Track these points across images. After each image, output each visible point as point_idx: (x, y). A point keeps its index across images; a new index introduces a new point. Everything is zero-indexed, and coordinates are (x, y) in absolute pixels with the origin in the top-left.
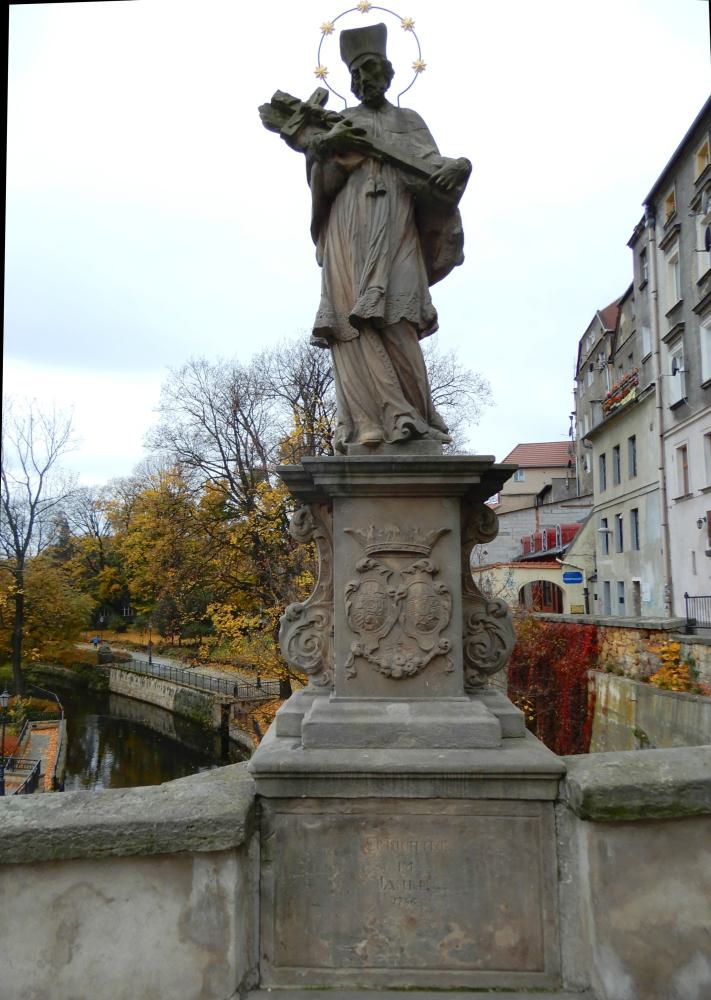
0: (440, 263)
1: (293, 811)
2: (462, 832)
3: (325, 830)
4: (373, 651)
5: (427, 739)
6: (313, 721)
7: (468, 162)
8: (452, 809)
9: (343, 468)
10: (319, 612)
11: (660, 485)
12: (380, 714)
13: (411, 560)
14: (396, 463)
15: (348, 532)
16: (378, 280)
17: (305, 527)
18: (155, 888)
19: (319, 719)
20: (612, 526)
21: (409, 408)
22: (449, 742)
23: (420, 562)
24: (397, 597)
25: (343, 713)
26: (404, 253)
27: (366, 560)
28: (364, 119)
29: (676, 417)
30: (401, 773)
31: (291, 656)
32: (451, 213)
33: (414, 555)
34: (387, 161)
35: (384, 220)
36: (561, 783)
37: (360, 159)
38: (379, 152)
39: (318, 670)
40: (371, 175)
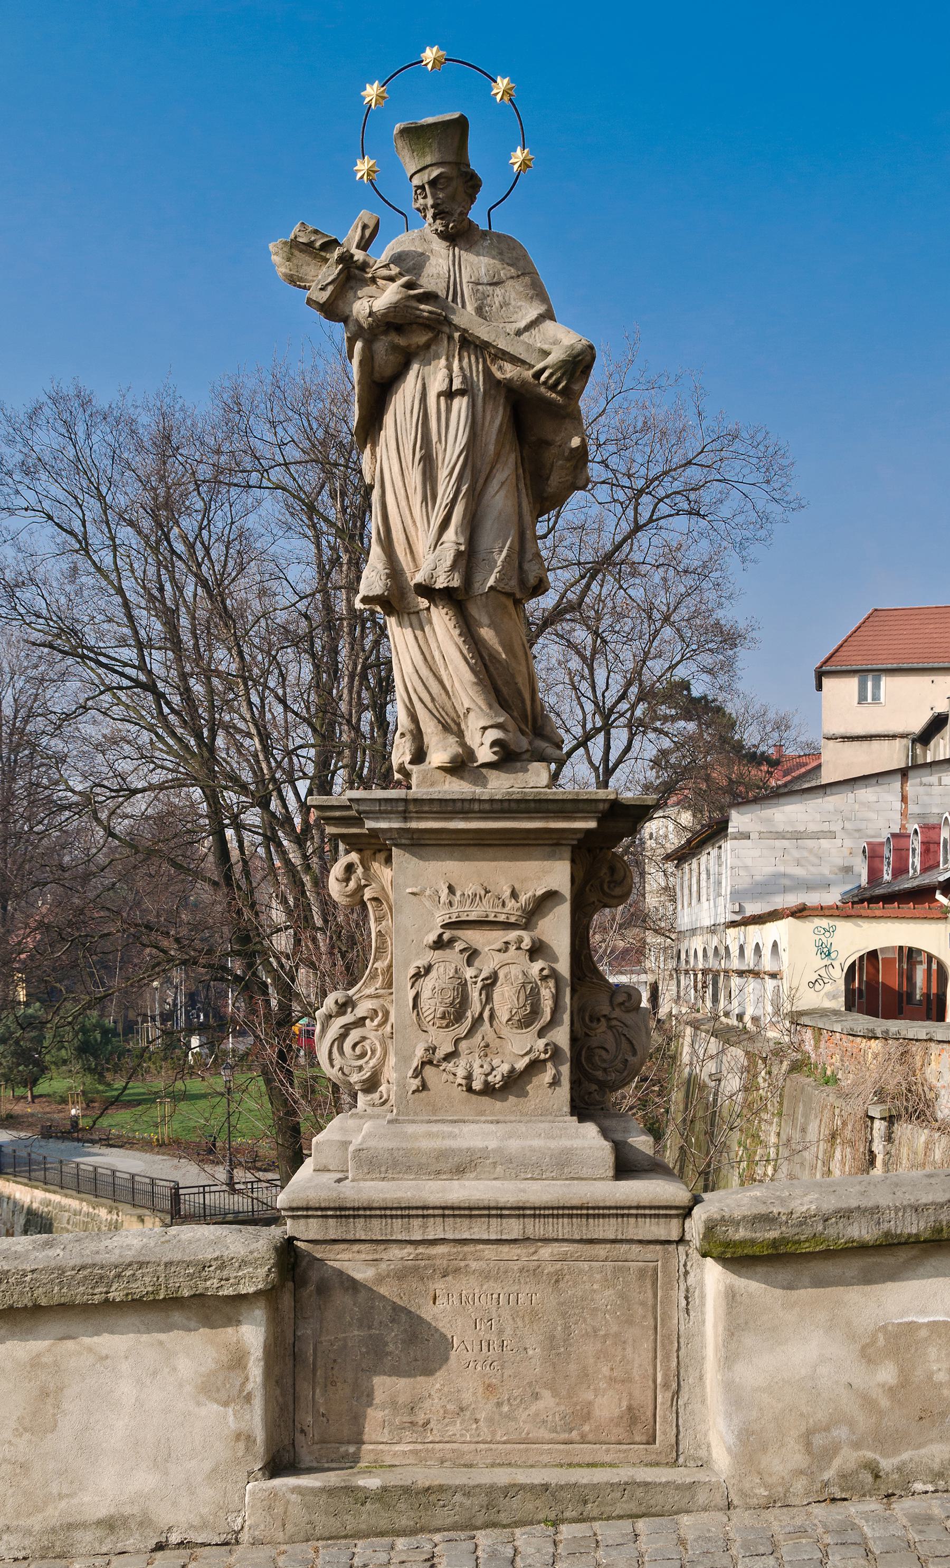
13: (501, 933)
14: (480, 801)
15: (413, 894)
17: (352, 884)
39: (371, 1085)
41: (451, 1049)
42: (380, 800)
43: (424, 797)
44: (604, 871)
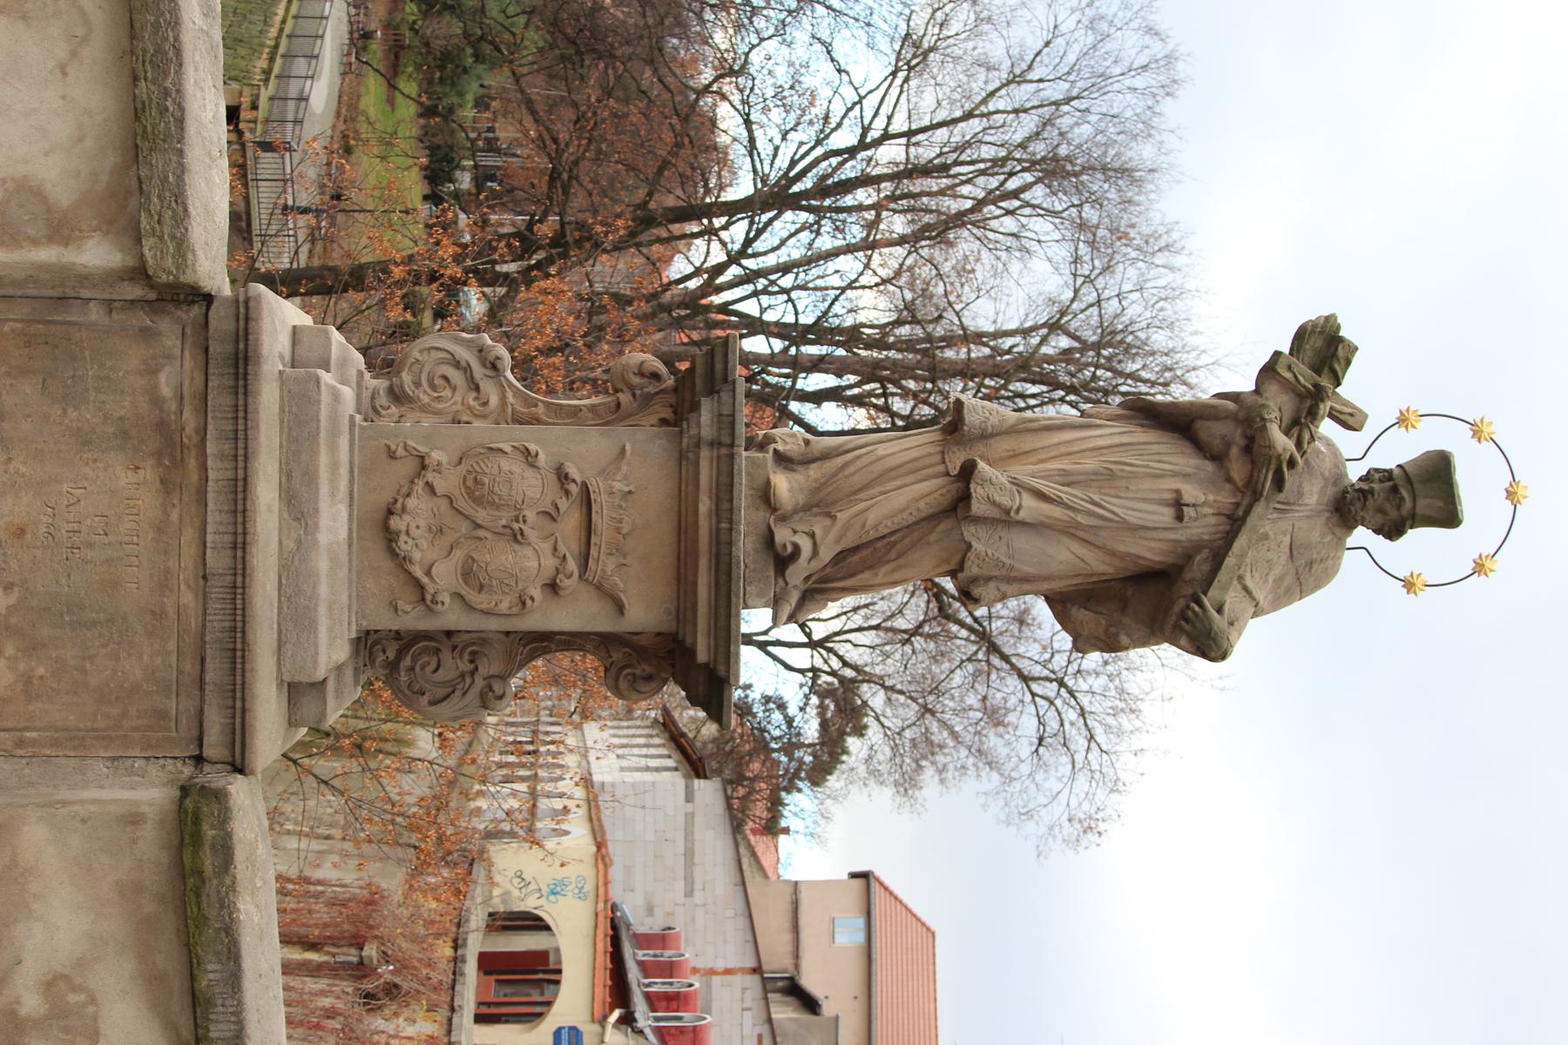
0: (1079, 614)
1: (187, 353)
2: (153, 613)
3: (157, 401)
4: (430, 488)
5: (294, 570)
6: (323, 388)
7: (1223, 657)
8: (188, 599)
9: (724, 445)
10: (494, 400)
12: (333, 494)
14: (731, 530)
15: (623, 451)
16: (1030, 507)
17: (636, 380)
18: (81, 140)
19: (325, 397)
21: (826, 555)
22: (289, 598)
23: (572, 565)
24: (516, 526)
25: (334, 434)
26: (1082, 551)
27: (579, 480)
28: (1316, 489)
30: (244, 523)
31: (421, 351)
32: (1156, 629)
33: (584, 559)
34: (1235, 522)
35: (1132, 517)
36: (229, 767)
37: (1240, 484)
38: (1247, 513)
39: (397, 396)
40: (1211, 497)
41: (439, 491)
42: (733, 415)
43: (736, 467)
44: (648, 669)
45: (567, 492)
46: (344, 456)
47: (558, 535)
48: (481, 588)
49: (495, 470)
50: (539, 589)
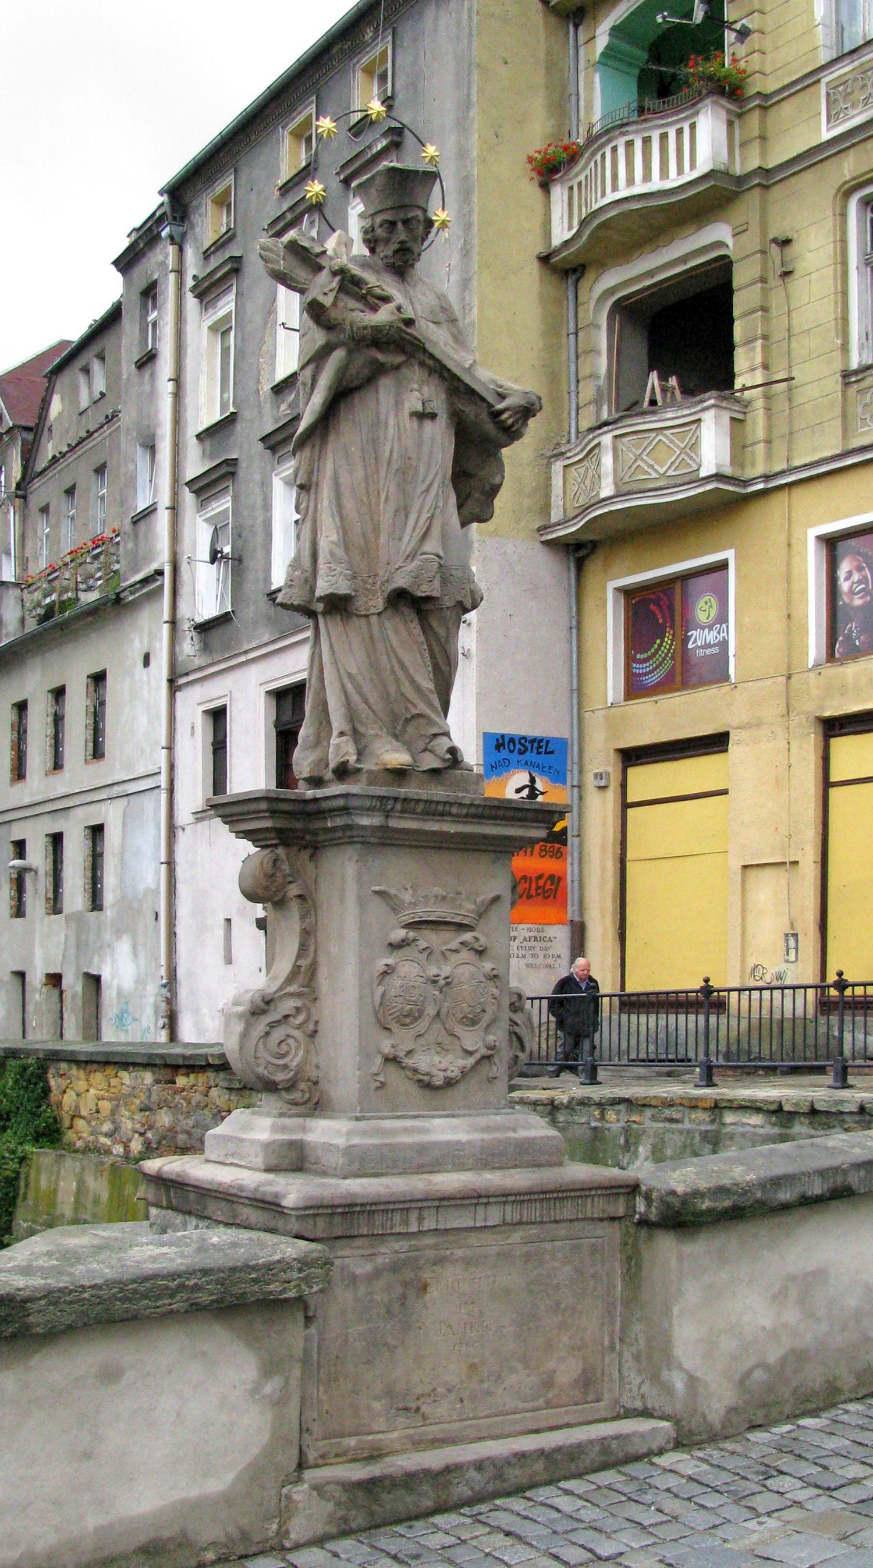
4: (409, 1053)
11: (163, 780)
20: (37, 856)
23: (467, 936)
24: (442, 982)
29: (206, 648)
33: (461, 927)
45: (414, 940)
46: (398, 1124)
47: (444, 948)
48: (484, 1011)
49: (399, 1000)
50: (483, 964)
